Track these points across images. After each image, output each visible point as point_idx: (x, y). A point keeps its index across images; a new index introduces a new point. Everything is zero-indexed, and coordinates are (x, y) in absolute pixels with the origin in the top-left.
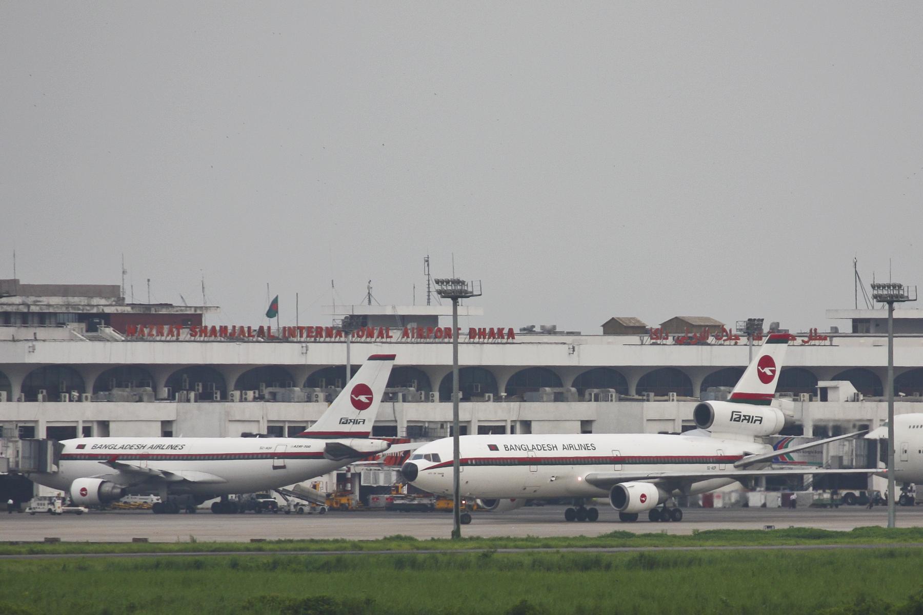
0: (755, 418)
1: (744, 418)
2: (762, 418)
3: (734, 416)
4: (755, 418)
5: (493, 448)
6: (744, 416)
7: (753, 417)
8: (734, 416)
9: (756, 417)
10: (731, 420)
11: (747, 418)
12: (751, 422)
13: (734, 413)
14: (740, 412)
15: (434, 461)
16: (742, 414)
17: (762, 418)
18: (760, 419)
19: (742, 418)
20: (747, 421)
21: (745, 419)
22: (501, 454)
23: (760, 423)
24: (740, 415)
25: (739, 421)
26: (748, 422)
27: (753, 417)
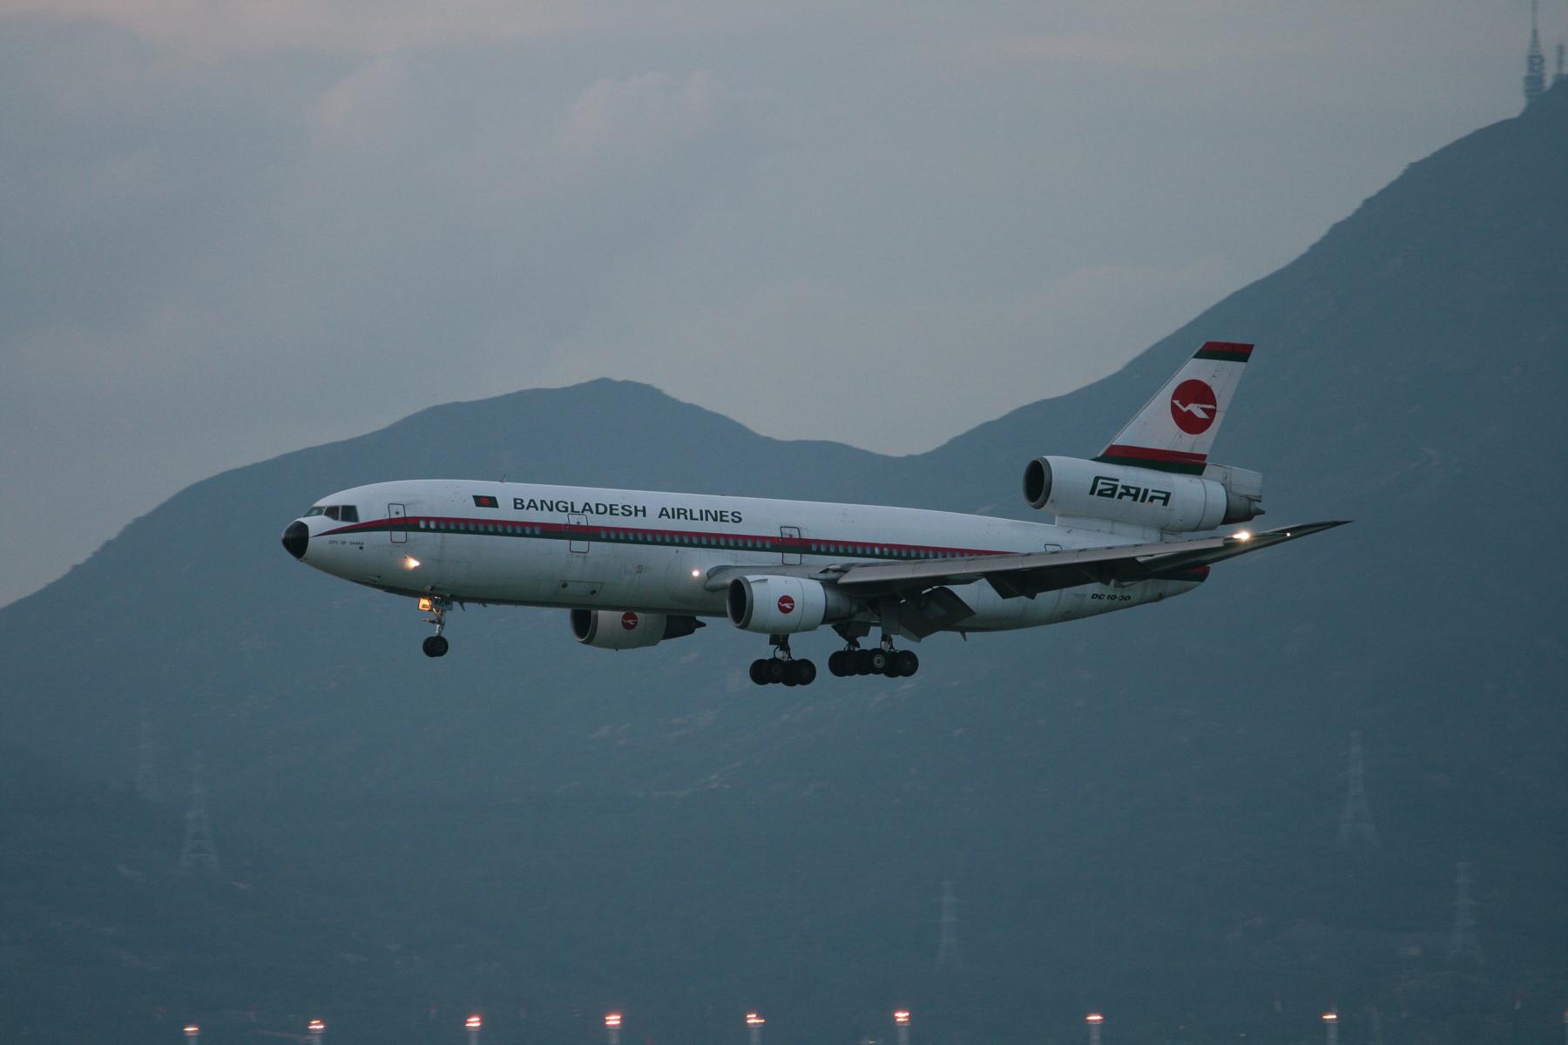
0: (1150, 494)
1: (1124, 491)
2: (1168, 495)
3: (1100, 487)
4: (1150, 494)
5: (490, 502)
6: (1127, 488)
7: (1146, 491)
8: (1100, 487)
9: (1153, 491)
10: (1092, 492)
11: (1133, 491)
12: (1143, 500)
13: (1100, 481)
14: (1117, 480)
15: (344, 519)
16: (1120, 484)
17: (1168, 495)
18: (1164, 495)
20: (1132, 498)
21: (1128, 494)
22: (505, 512)
23: (1165, 504)
24: (1115, 487)
25: (1112, 496)
27: (1146, 491)
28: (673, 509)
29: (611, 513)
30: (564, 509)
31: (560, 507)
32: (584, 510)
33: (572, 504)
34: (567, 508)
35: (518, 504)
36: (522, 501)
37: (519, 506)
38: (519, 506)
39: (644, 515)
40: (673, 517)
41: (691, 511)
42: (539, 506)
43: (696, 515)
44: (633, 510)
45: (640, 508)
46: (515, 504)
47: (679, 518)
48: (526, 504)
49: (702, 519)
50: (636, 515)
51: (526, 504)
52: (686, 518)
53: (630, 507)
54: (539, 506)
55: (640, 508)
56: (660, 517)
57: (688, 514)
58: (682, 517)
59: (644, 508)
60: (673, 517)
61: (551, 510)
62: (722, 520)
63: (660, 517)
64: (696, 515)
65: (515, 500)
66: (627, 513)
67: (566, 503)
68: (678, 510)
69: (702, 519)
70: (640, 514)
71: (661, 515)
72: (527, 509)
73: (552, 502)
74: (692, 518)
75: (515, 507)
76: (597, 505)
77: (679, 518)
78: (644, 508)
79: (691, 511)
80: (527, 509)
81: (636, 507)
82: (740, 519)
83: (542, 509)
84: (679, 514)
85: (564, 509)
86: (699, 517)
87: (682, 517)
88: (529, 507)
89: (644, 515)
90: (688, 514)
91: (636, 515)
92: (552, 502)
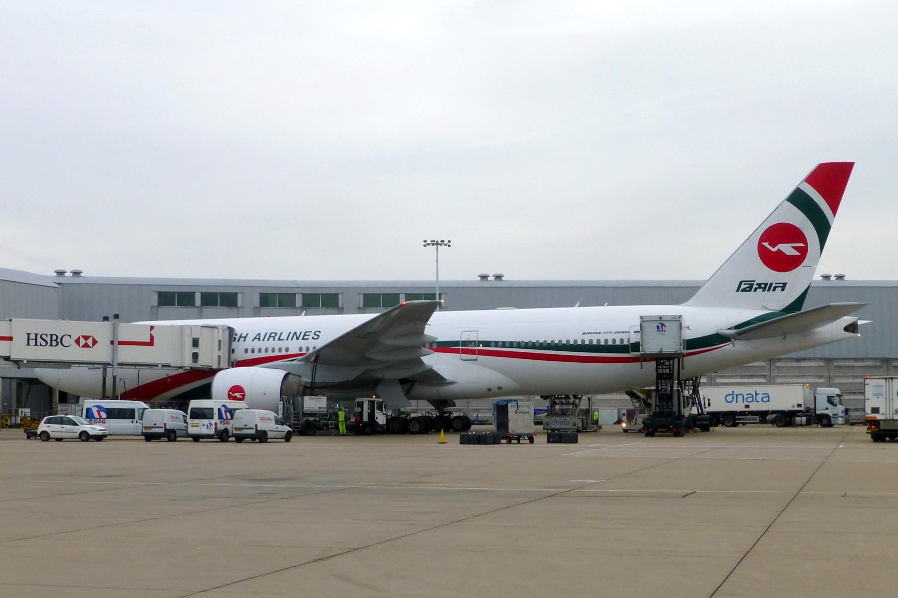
6: (757, 284)
11: (763, 286)
19: (755, 286)
21: (761, 288)
26: (764, 290)
40: (263, 340)
41: (282, 333)
43: (284, 337)
47: (268, 340)
49: (287, 339)
56: (253, 341)
57: (277, 338)
58: (272, 339)
59: (247, 334)
60: (263, 340)
62: (303, 339)
63: (253, 341)
64: (284, 337)
68: (271, 333)
69: (287, 339)
70: (242, 339)
71: (255, 338)
78: (247, 334)
79: (282, 333)
81: (241, 334)
84: (270, 336)
87: (272, 339)
90: (277, 338)
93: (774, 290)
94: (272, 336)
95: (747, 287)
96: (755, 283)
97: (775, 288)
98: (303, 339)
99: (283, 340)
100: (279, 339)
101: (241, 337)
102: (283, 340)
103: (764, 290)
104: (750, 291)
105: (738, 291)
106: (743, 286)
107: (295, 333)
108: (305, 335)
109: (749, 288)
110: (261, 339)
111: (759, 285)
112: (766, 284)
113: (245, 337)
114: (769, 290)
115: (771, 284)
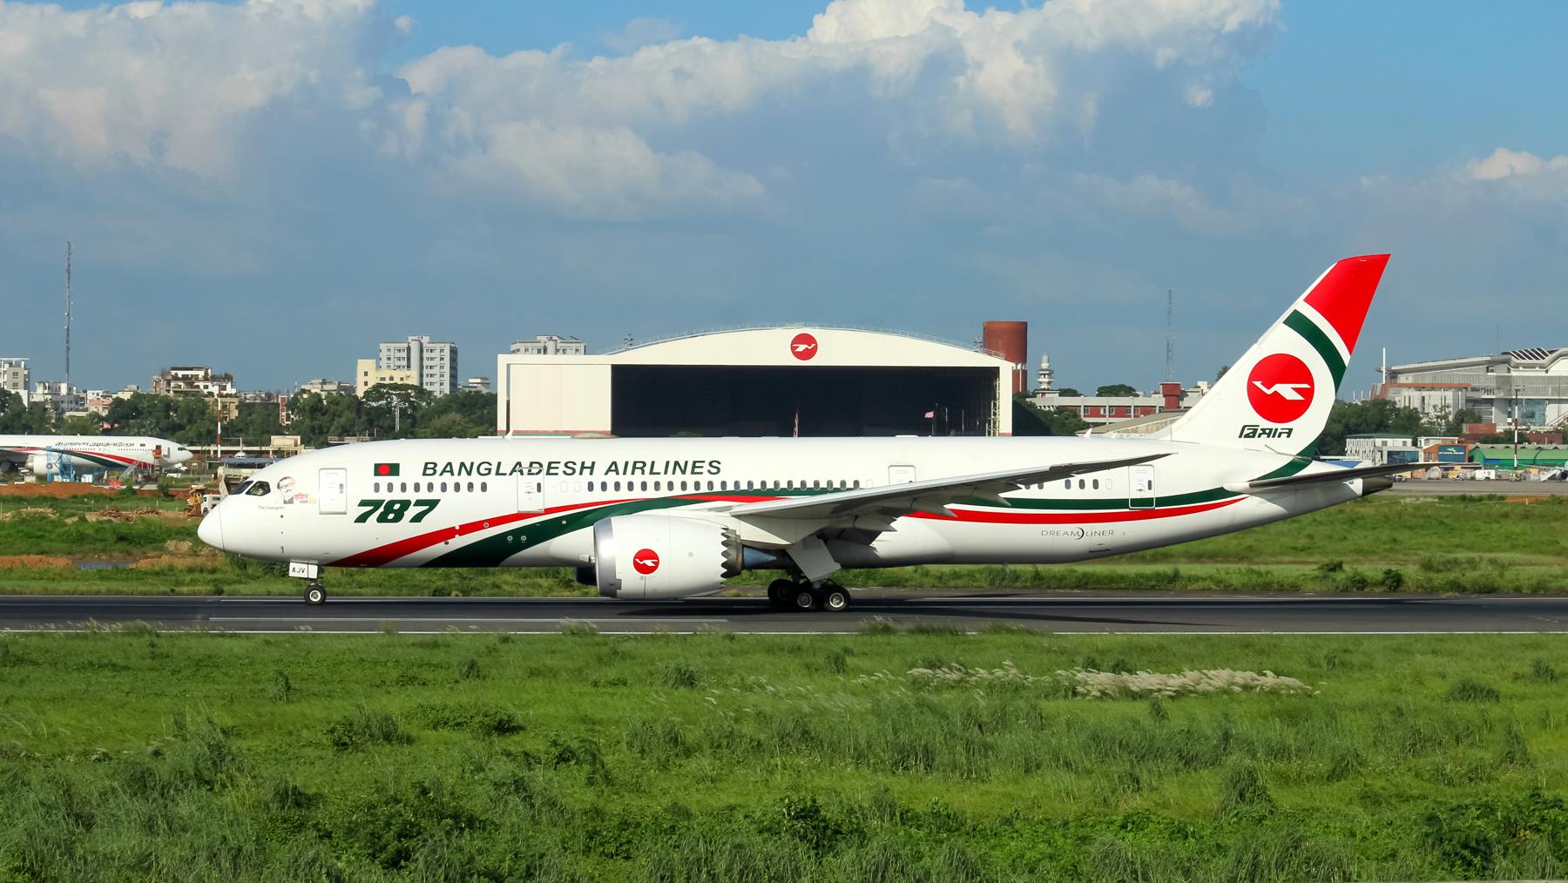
11: (1267, 431)
19: (1259, 431)
21: (1264, 433)
26: (1269, 437)
28: (627, 463)
29: (548, 473)
30: (487, 471)
31: (482, 470)
32: (514, 470)
33: (499, 464)
34: (490, 470)
35: (429, 468)
36: (435, 465)
37: (428, 472)
38: (428, 472)
39: (591, 474)
40: (625, 473)
41: (653, 463)
42: (456, 470)
43: (659, 468)
44: (578, 468)
45: (588, 464)
46: (426, 468)
47: (633, 473)
48: (439, 469)
49: (666, 473)
50: (581, 473)
51: (439, 469)
52: (643, 473)
53: (575, 464)
54: (456, 470)
55: (588, 464)
56: (606, 474)
57: (647, 469)
58: (638, 472)
59: (593, 463)
60: (625, 473)
61: (469, 473)
62: (693, 473)
63: (606, 474)
64: (659, 468)
65: (427, 464)
66: (570, 471)
67: (490, 464)
68: (635, 463)
69: (666, 473)
70: (586, 472)
71: (609, 470)
72: (441, 474)
73: (472, 464)
74: (651, 473)
75: (424, 474)
76: (531, 464)
77: (633, 473)
78: (593, 463)
79: (653, 463)
80: (441, 474)
81: (583, 463)
82: (718, 469)
83: (459, 474)
84: (634, 468)
85: (487, 471)
86: (663, 472)
87: (638, 472)
88: (444, 471)
89: (591, 474)
90: (647, 469)
91: (581, 473)
92: (472, 464)
93: (1279, 436)
94: (639, 466)
95: (1250, 432)
96: (1259, 428)
97: (1281, 433)
98: (693, 473)
99: (659, 473)
100: (651, 473)
101: (583, 467)
102: (659, 473)
103: (1269, 437)
104: (1253, 436)
105: (1240, 437)
106: (1246, 432)
107: (677, 463)
108: (694, 467)
109: (1253, 434)
110: (621, 470)
111: (1263, 430)
112: (1271, 430)
113: (592, 468)
114: (1274, 436)
115: (1276, 429)
